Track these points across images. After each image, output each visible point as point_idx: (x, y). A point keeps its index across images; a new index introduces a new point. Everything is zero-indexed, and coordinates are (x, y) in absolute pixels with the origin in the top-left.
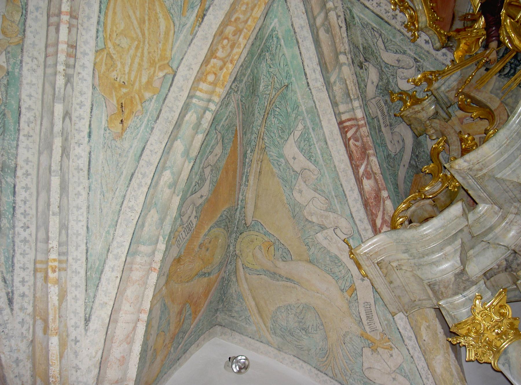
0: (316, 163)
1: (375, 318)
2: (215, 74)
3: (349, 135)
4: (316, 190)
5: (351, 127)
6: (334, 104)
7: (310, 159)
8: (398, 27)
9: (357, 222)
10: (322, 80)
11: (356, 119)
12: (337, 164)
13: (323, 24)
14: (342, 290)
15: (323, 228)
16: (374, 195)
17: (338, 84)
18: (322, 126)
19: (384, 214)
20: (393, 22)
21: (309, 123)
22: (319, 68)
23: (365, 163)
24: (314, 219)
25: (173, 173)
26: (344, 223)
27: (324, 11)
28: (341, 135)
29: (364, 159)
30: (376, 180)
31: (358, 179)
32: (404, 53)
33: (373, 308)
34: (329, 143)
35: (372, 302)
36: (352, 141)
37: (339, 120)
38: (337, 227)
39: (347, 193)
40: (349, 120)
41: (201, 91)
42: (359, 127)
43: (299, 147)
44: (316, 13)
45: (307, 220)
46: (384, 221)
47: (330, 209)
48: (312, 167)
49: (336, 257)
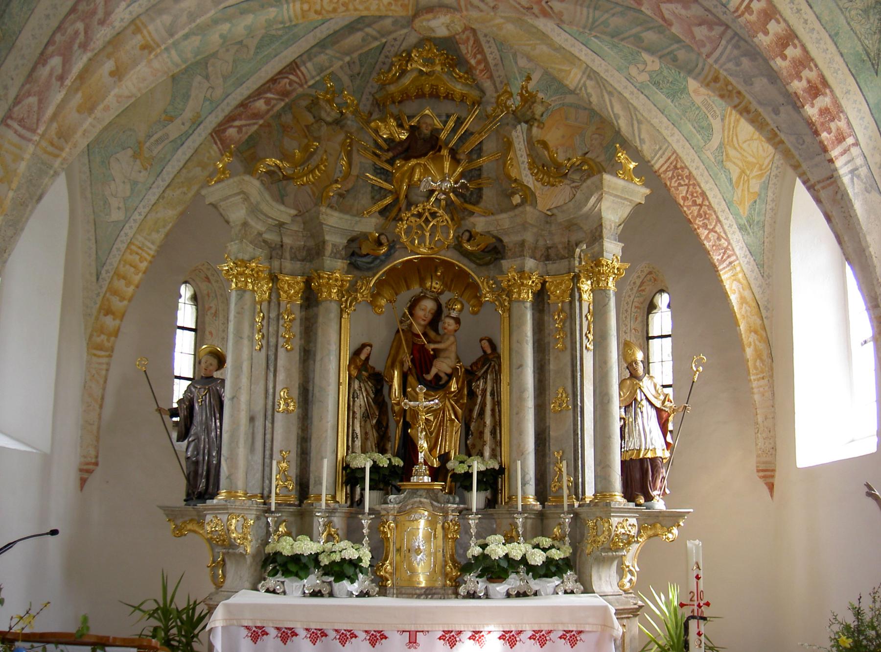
0: (256, 53)
1: (160, 147)
2: (310, 9)
3: (291, 77)
4: (234, 61)
5: (297, 76)
6: (309, 54)
7: (257, 48)
8: (380, 60)
9: (225, 102)
10: (323, 36)
11: (306, 82)
12: (263, 69)
13: (367, 34)
14: (165, 111)
15: (207, 77)
16: (256, 111)
17: (326, 57)
18: (287, 48)
19: (245, 125)
20: (382, 56)
21: (285, 38)
22: (331, 32)
23: (277, 97)
24: (210, 69)
25: (230, 30)
26: (218, 92)
27: (378, 36)
28: (288, 66)
29: (278, 94)
30: (268, 111)
31: (260, 94)
32: (361, 66)
33: (166, 142)
34: (277, 59)
35: (171, 138)
36: (287, 80)
37: (298, 61)
38: (213, 88)
39: (244, 85)
40: (302, 73)
41: (294, 6)
42: (301, 86)
43: (263, 37)
44: (374, 26)
45: (207, 63)
46: (240, 128)
47: (225, 78)
48: (252, 52)
49: (189, 96)
